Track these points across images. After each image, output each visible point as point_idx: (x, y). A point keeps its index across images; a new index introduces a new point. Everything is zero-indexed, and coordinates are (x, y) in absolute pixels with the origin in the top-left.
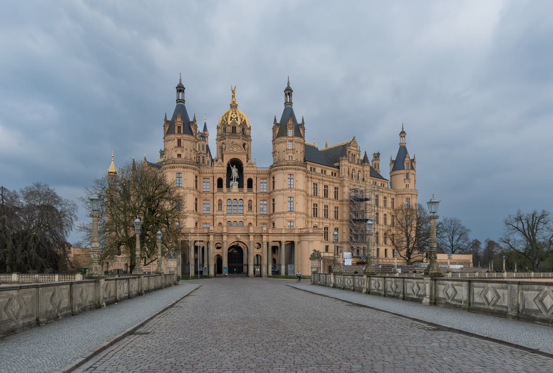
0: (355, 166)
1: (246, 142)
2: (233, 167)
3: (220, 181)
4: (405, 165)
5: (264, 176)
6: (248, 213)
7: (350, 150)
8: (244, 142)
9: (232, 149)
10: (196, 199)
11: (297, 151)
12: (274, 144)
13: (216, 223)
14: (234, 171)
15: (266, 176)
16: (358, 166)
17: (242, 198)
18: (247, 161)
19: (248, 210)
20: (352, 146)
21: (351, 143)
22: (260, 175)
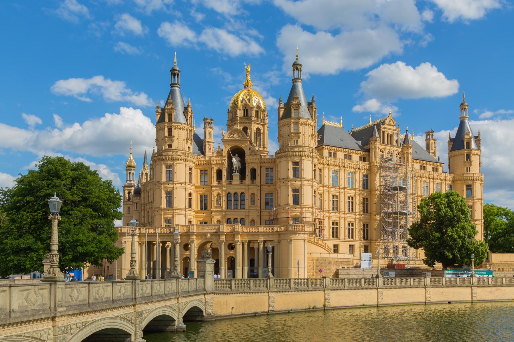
0: (392, 148)
1: (261, 127)
2: (234, 155)
3: (219, 173)
4: (465, 144)
5: (269, 164)
6: (250, 208)
7: (383, 130)
8: (257, 126)
9: (232, 135)
10: (190, 195)
11: (304, 135)
12: (279, 127)
13: (214, 221)
14: (234, 160)
15: (272, 164)
16: (396, 149)
17: (244, 191)
18: (250, 149)
19: (250, 205)
20: (388, 125)
21: (386, 121)
22: (264, 165)
